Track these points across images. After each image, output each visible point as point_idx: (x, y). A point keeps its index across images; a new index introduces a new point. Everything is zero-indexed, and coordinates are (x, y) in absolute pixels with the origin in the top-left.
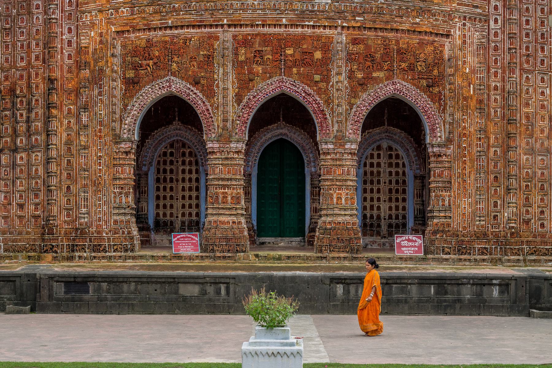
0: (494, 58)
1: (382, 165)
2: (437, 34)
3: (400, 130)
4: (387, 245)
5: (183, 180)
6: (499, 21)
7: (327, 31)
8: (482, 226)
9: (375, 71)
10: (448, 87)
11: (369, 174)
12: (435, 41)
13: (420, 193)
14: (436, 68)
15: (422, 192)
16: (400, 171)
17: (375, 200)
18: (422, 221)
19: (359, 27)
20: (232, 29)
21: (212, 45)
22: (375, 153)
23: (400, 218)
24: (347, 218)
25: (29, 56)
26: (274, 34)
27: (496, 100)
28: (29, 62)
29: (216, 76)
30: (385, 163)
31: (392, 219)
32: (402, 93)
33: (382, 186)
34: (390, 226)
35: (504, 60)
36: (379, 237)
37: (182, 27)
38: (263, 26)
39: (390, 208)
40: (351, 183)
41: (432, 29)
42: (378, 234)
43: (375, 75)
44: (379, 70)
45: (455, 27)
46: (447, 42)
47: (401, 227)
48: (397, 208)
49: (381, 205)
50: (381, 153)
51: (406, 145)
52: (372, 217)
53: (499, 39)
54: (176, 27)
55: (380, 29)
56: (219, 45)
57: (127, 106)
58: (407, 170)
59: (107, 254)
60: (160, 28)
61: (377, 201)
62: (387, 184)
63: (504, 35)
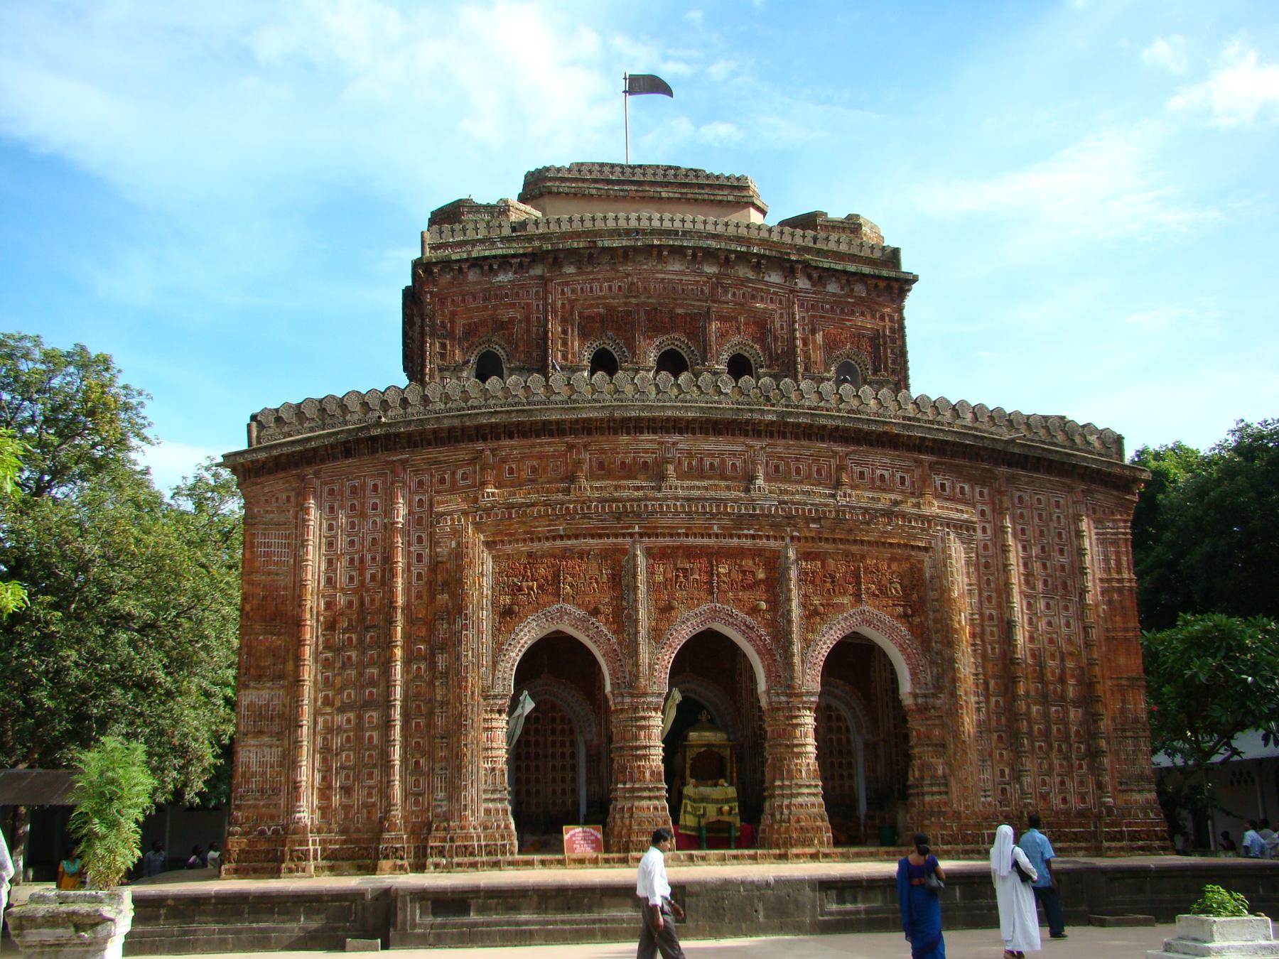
2: (913, 547)
5: (554, 755)
6: (989, 531)
7: (772, 543)
8: (990, 804)
10: (931, 615)
19: (813, 538)
20: (646, 539)
21: (619, 562)
24: (812, 799)
25: (362, 574)
26: (702, 546)
27: (992, 632)
28: (362, 582)
29: (624, 603)
37: (577, 537)
38: (687, 535)
46: (926, 558)
53: (990, 553)
54: (569, 538)
55: (841, 540)
56: (628, 561)
57: (502, 644)
59: (477, 859)
60: (547, 539)
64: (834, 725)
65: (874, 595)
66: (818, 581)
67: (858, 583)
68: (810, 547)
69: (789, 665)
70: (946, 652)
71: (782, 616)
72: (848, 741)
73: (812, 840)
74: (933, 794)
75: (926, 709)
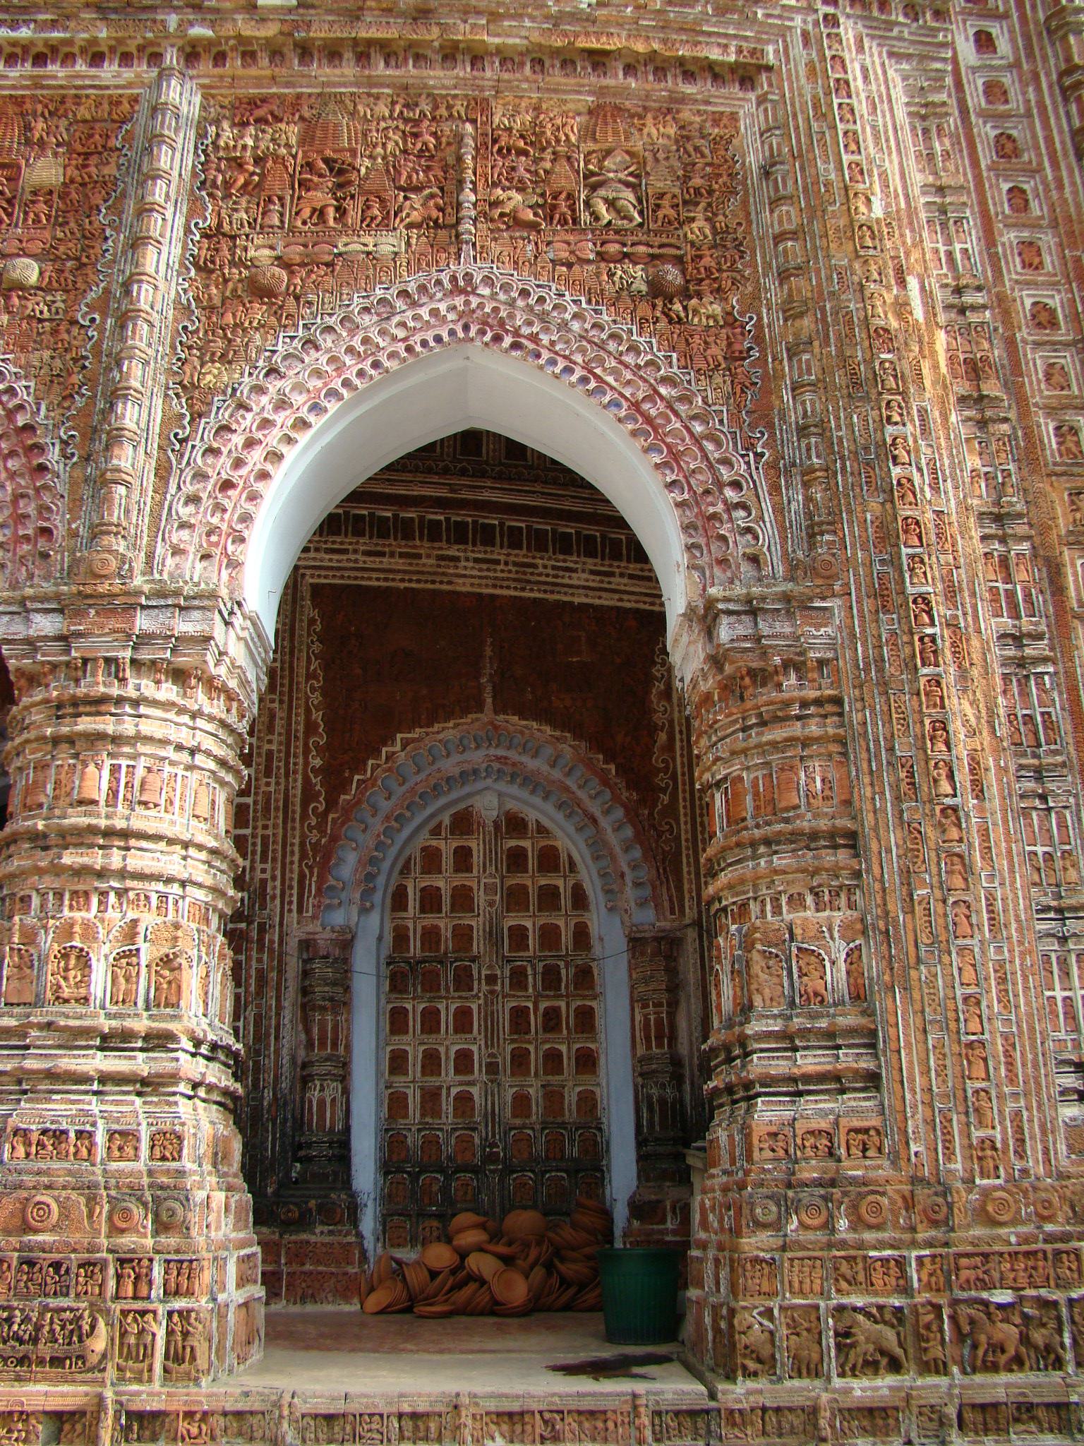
0: (1005, 187)
1: (481, 898)
3: (555, 727)
7: (110, 72)
9: (346, 229)
10: (774, 292)
12: (683, 100)
13: (659, 1022)
14: (699, 213)
15: (672, 1015)
16: (564, 924)
22: (447, 847)
32: (508, 341)
35: (1060, 187)
40: (171, 862)
41: (664, 41)
43: (352, 245)
44: (368, 223)
45: (783, 32)
46: (746, 109)
49: (475, 1091)
50: (473, 844)
51: (581, 794)
53: (1016, 102)
61: (458, 1071)
63: (1038, 89)
64: (532, 881)
65: (515, 222)
66: (277, 184)
67: (451, 179)
68: (255, 78)
69: (98, 485)
70: (850, 425)
71: (103, 305)
72: (582, 936)
73: (78, 1332)
74: (797, 1086)
75: (761, 677)
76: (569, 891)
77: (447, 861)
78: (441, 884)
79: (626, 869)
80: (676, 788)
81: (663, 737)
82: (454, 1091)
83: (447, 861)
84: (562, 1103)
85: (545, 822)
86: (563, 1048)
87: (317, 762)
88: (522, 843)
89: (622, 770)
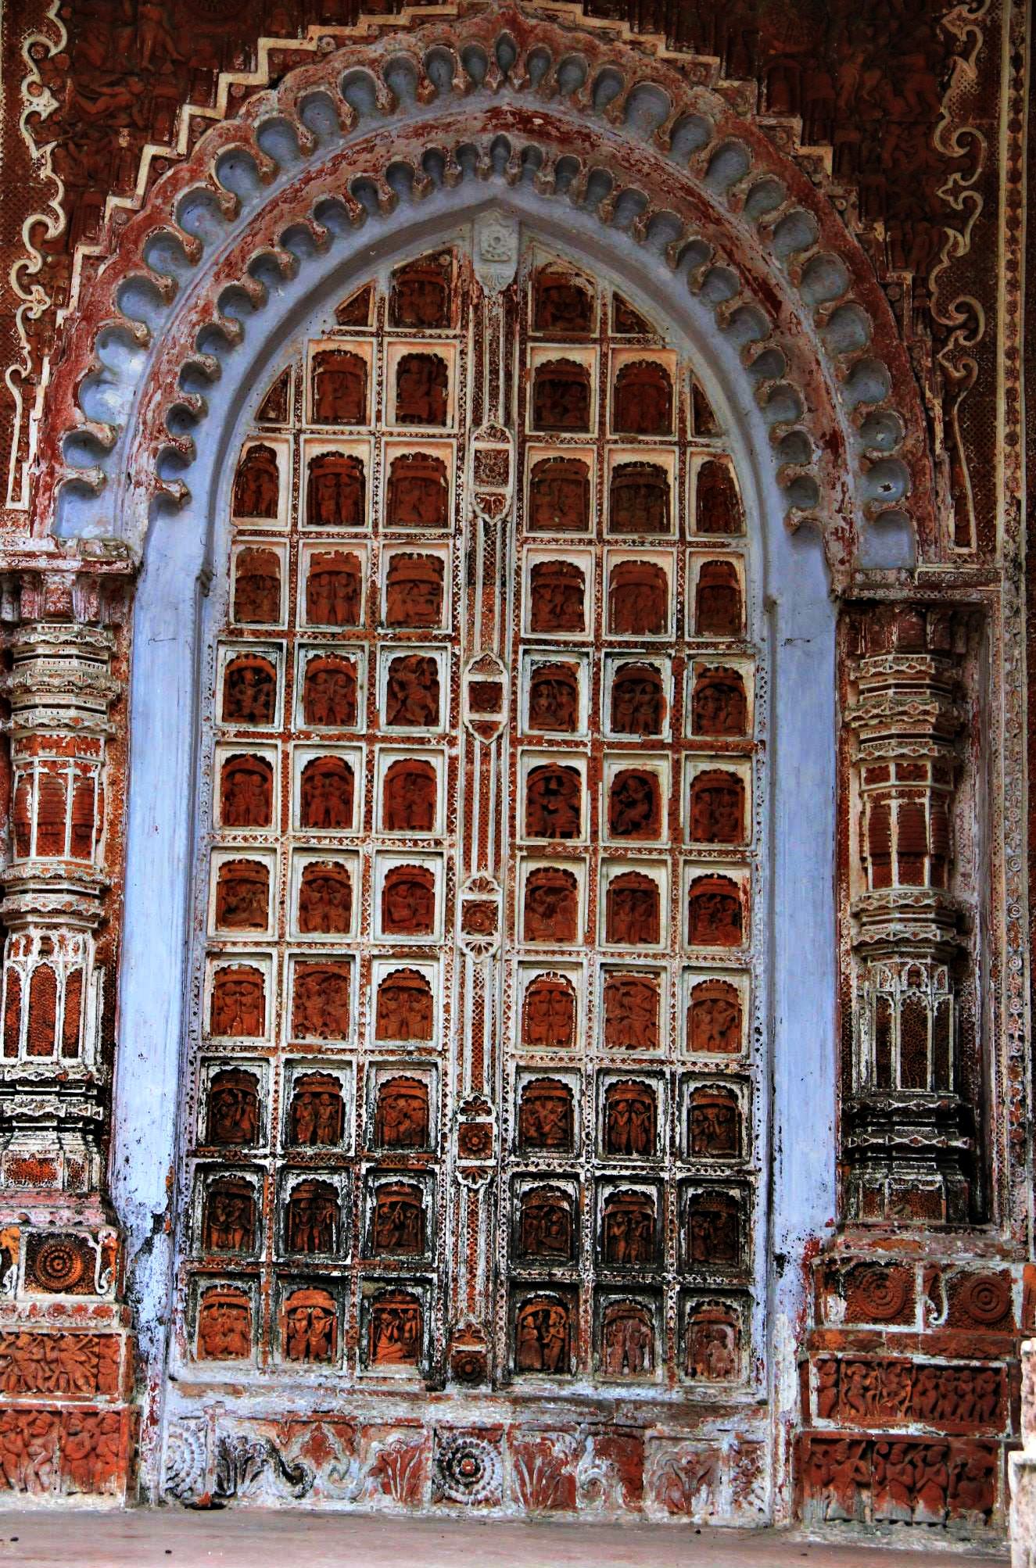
1: (464, 490)
3: (678, 39)
4: (500, 1471)
11: (294, 600)
13: (911, 817)
15: (944, 801)
16: (678, 570)
17: (368, 905)
18: (944, 1158)
22: (383, 357)
23: (670, 1126)
30: (491, 468)
31: (565, 1142)
33: (445, 745)
34: (541, 1228)
36: (402, 1375)
39: (548, 1013)
42: (393, 1325)
47: (677, 1243)
48: (631, 1006)
49: (433, 972)
50: (448, 353)
51: (742, 227)
52: (316, 1106)
58: (763, 557)
61: (391, 923)
62: (516, 710)
64: (599, 452)
72: (719, 599)
76: (692, 483)
77: (382, 393)
78: (362, 451)
79: (844, 425)
80: (990, 213)
81: (967, 72)
82: (381, 971)
83: (382, 393)
84: (652, 1012)
85: (641, 304)
86: (661, 877)
87: (43, 104)
88: (578, 355)
89: (848, 164)
